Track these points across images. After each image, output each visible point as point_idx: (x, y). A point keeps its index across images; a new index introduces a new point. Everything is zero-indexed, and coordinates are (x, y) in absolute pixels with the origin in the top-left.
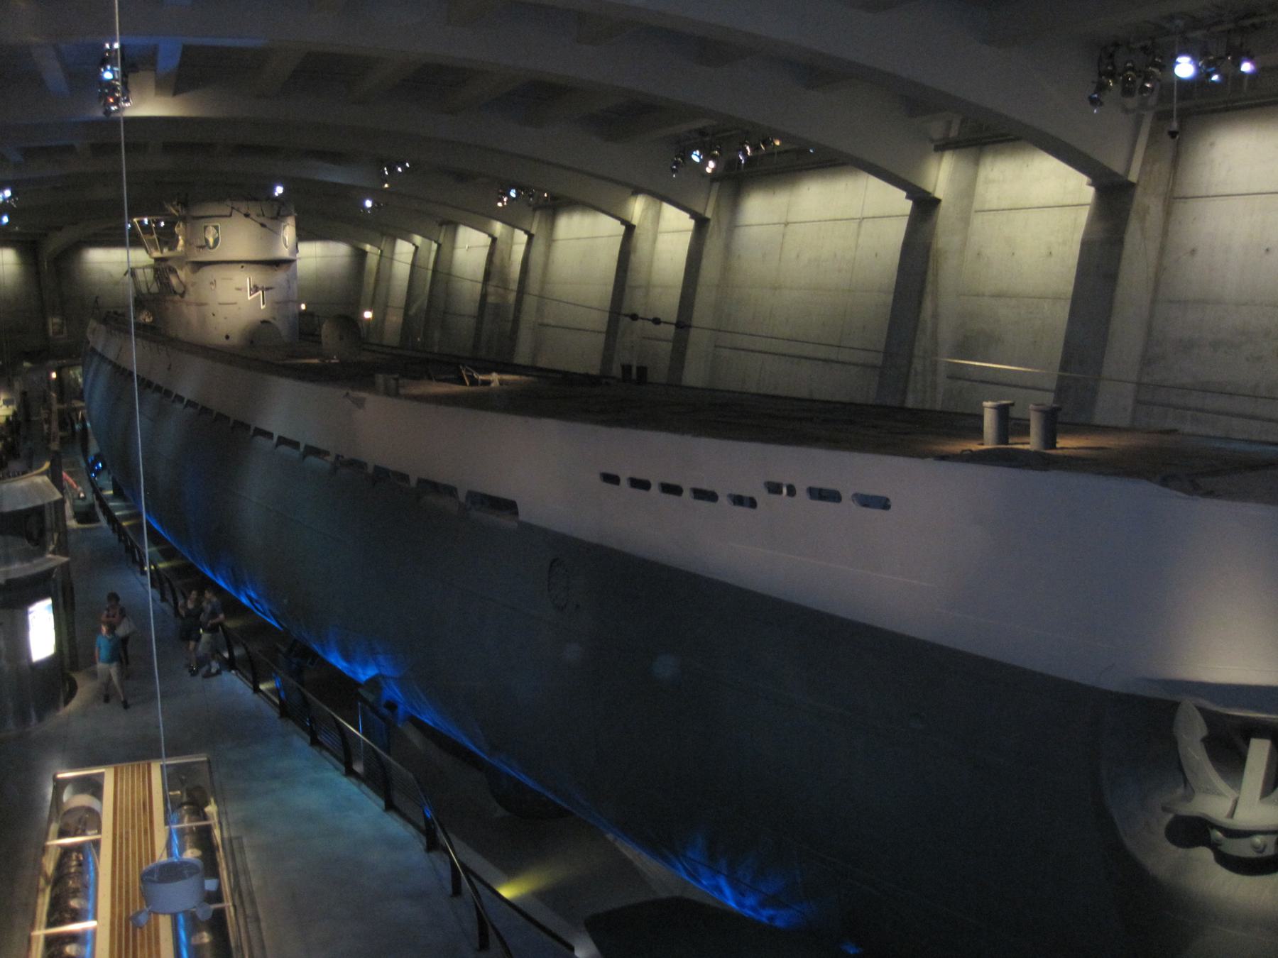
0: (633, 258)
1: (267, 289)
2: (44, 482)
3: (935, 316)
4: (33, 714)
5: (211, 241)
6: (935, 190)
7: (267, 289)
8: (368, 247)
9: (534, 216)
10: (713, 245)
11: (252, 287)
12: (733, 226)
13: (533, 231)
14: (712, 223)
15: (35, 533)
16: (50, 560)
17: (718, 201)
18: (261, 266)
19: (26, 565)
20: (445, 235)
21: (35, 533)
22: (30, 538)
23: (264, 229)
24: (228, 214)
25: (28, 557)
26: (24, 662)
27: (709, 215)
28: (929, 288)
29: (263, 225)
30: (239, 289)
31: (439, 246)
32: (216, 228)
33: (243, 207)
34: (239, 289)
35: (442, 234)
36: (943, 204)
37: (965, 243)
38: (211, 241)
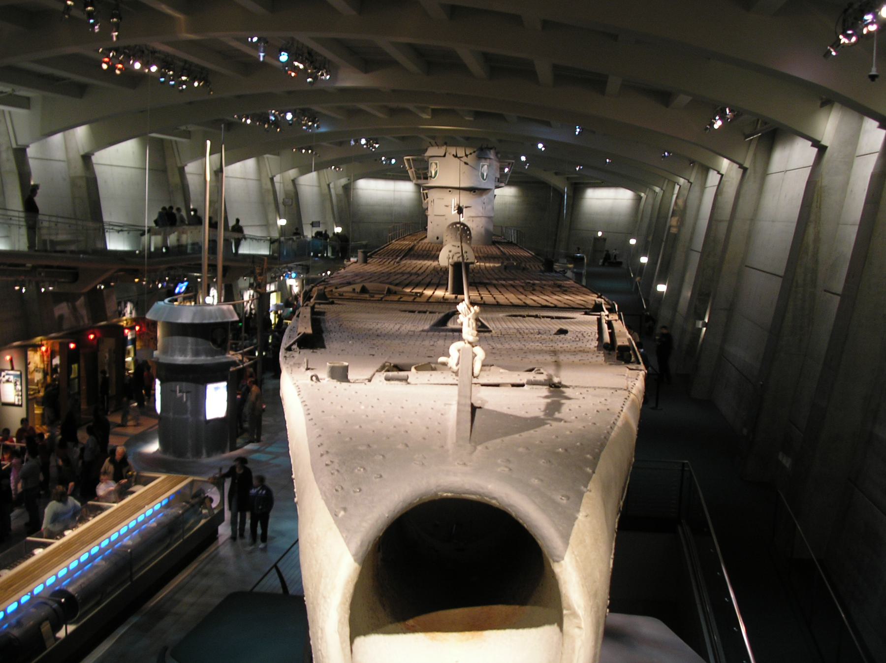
0: (719, 198)
1: (466, 207)
2: (229, 310)
3: (817, 240)
4: (204, 451)
5: (433, 173)
6: (822, 139)
7: (466, 207)
8: (643, 194)
9: (692, 170)
10: (751, 186)
11: (455, 205)
12: (765, 173)
13: (692, 180)
14: (748, 171)
15: (219, 341)
16: (228, 358)
17: (755, 154)
18: (468, 192)
19: (209, 358)
20: (667, 185)
21: (219, 341)
22: (214, 342)
23: (466, 166)
24: (443, 155)
25: (212, 353)
26: (202, 418)
27: (747, 165)
28: (812, 217)
29: (466, 163)
30: (447, 206)
31: (664, 191)
32: (436, 164)
33: (452, 150)
34: (447, 206)
35: (665, 185)
36: (828, 149)
37: (847, 182)
38: (433, 173)
